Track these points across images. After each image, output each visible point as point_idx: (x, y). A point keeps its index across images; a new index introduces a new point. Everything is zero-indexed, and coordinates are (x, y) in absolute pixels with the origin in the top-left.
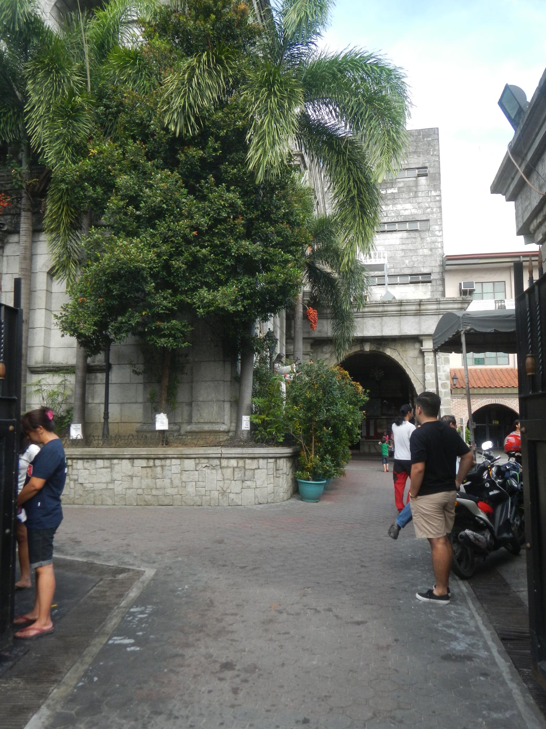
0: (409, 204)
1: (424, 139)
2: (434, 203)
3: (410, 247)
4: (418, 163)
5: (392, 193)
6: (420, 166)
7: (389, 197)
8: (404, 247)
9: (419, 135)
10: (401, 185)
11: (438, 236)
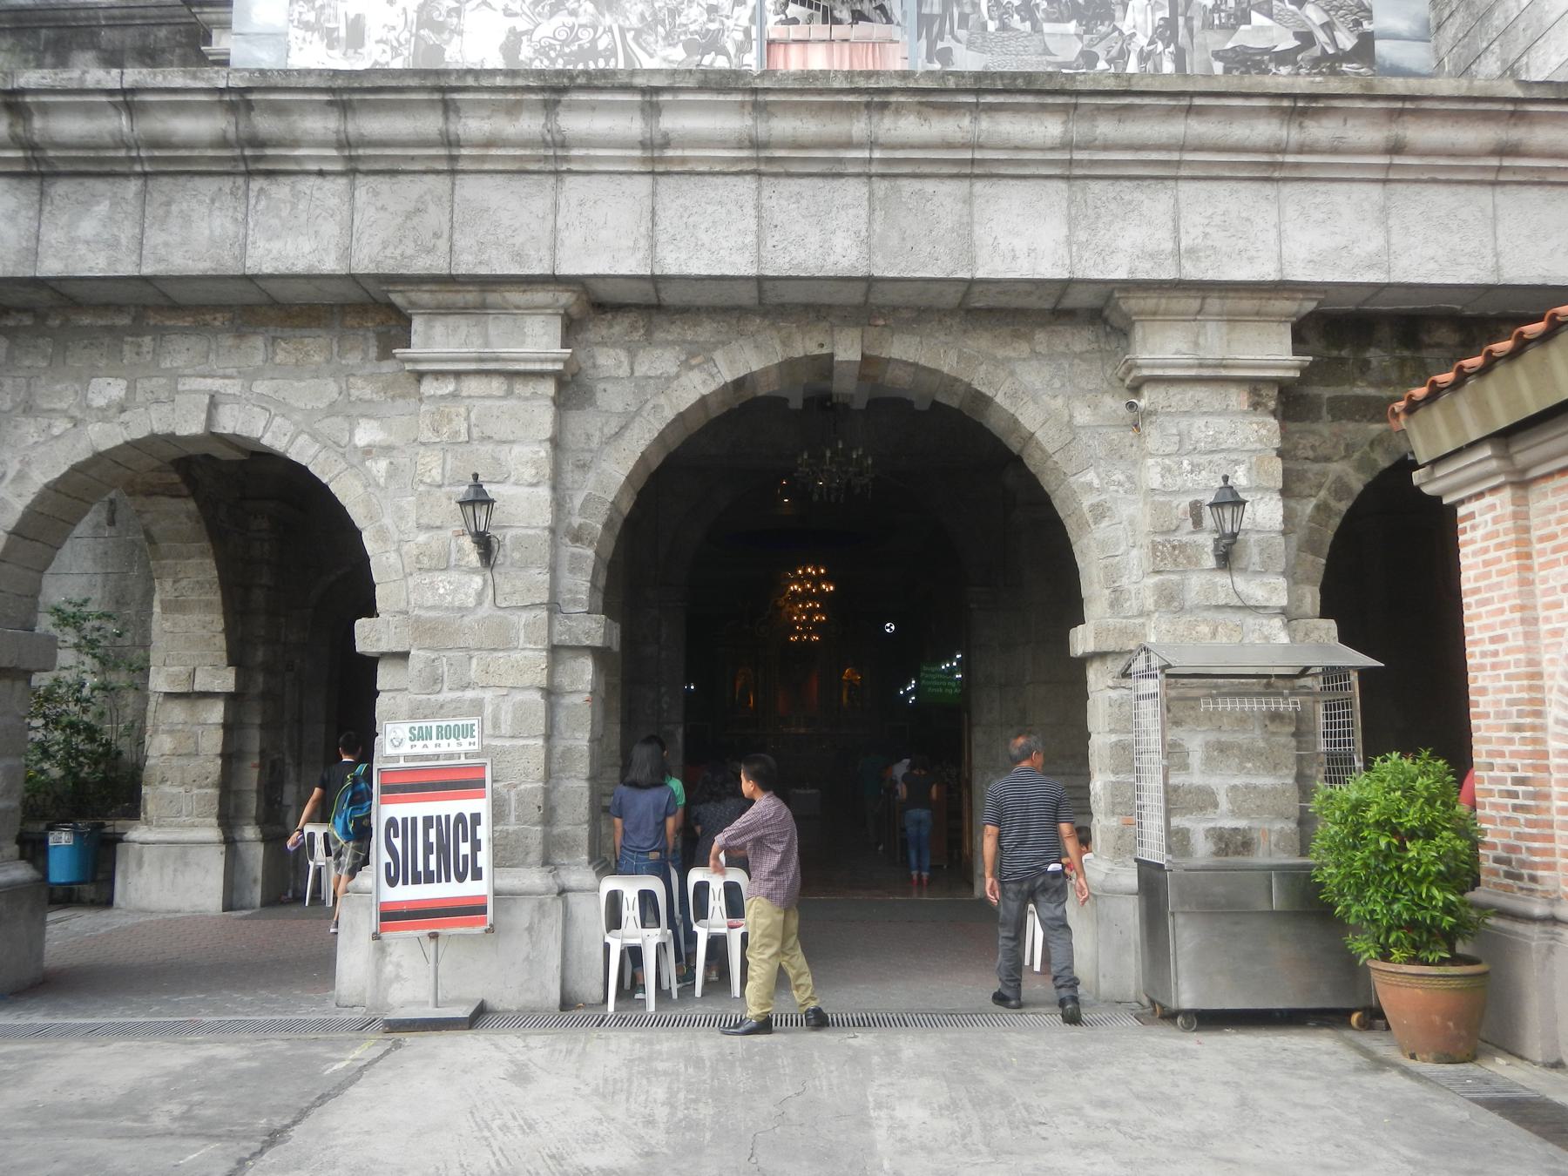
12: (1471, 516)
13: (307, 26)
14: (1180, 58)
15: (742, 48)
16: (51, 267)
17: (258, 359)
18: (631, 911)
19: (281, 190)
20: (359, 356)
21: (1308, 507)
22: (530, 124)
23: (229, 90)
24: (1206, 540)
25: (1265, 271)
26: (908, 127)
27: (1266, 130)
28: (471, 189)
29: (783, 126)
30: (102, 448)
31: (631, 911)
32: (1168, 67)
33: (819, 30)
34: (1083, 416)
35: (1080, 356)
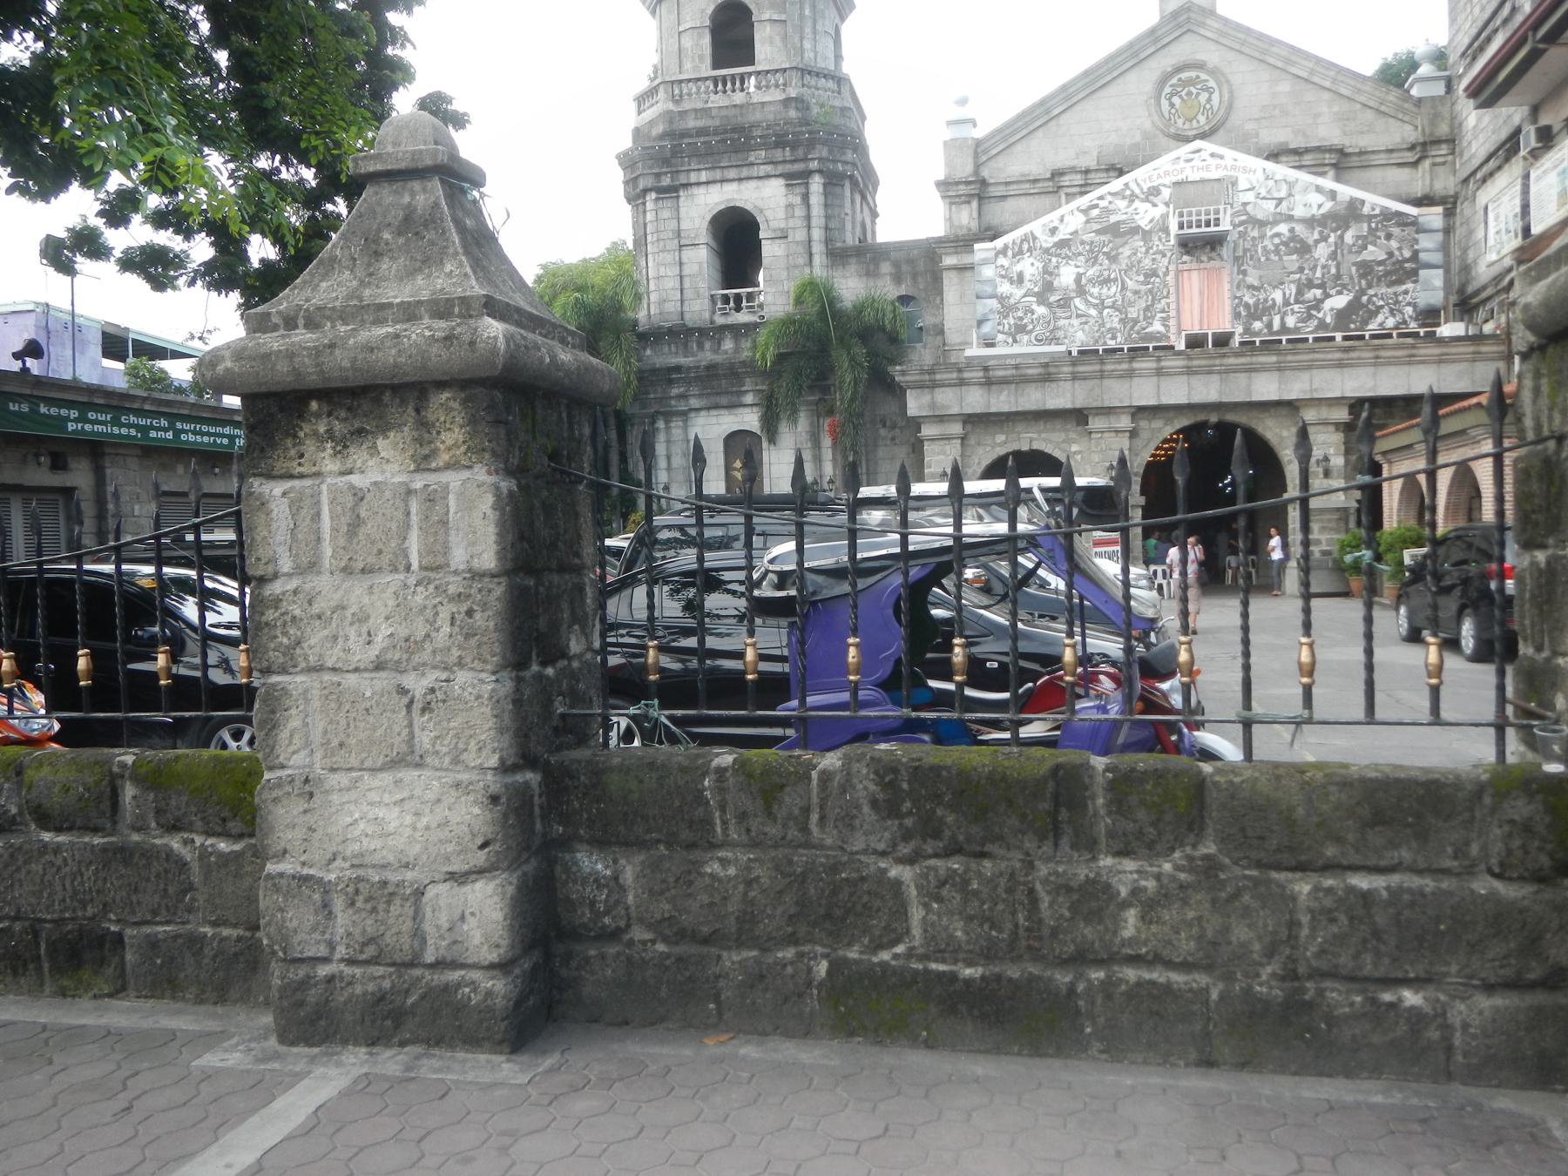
13: (1003, 277)
14: (1338, 267)
15: (1166, 273)
16: (993, 410)
18: (1160, 574)
19: (1054, 385)
20: (1071, 426)
21: (1354, 458)
22: (1125, 366)
24: (1321, 470)
25: (1337, 394)
26: (1232, 361)
27: (1338, 355)
28: (1106, 382)
29: (1196, 363)
31: (1160, 574)
32: (1333, 271)
33: (1194, 265)
34: (1285, 433)
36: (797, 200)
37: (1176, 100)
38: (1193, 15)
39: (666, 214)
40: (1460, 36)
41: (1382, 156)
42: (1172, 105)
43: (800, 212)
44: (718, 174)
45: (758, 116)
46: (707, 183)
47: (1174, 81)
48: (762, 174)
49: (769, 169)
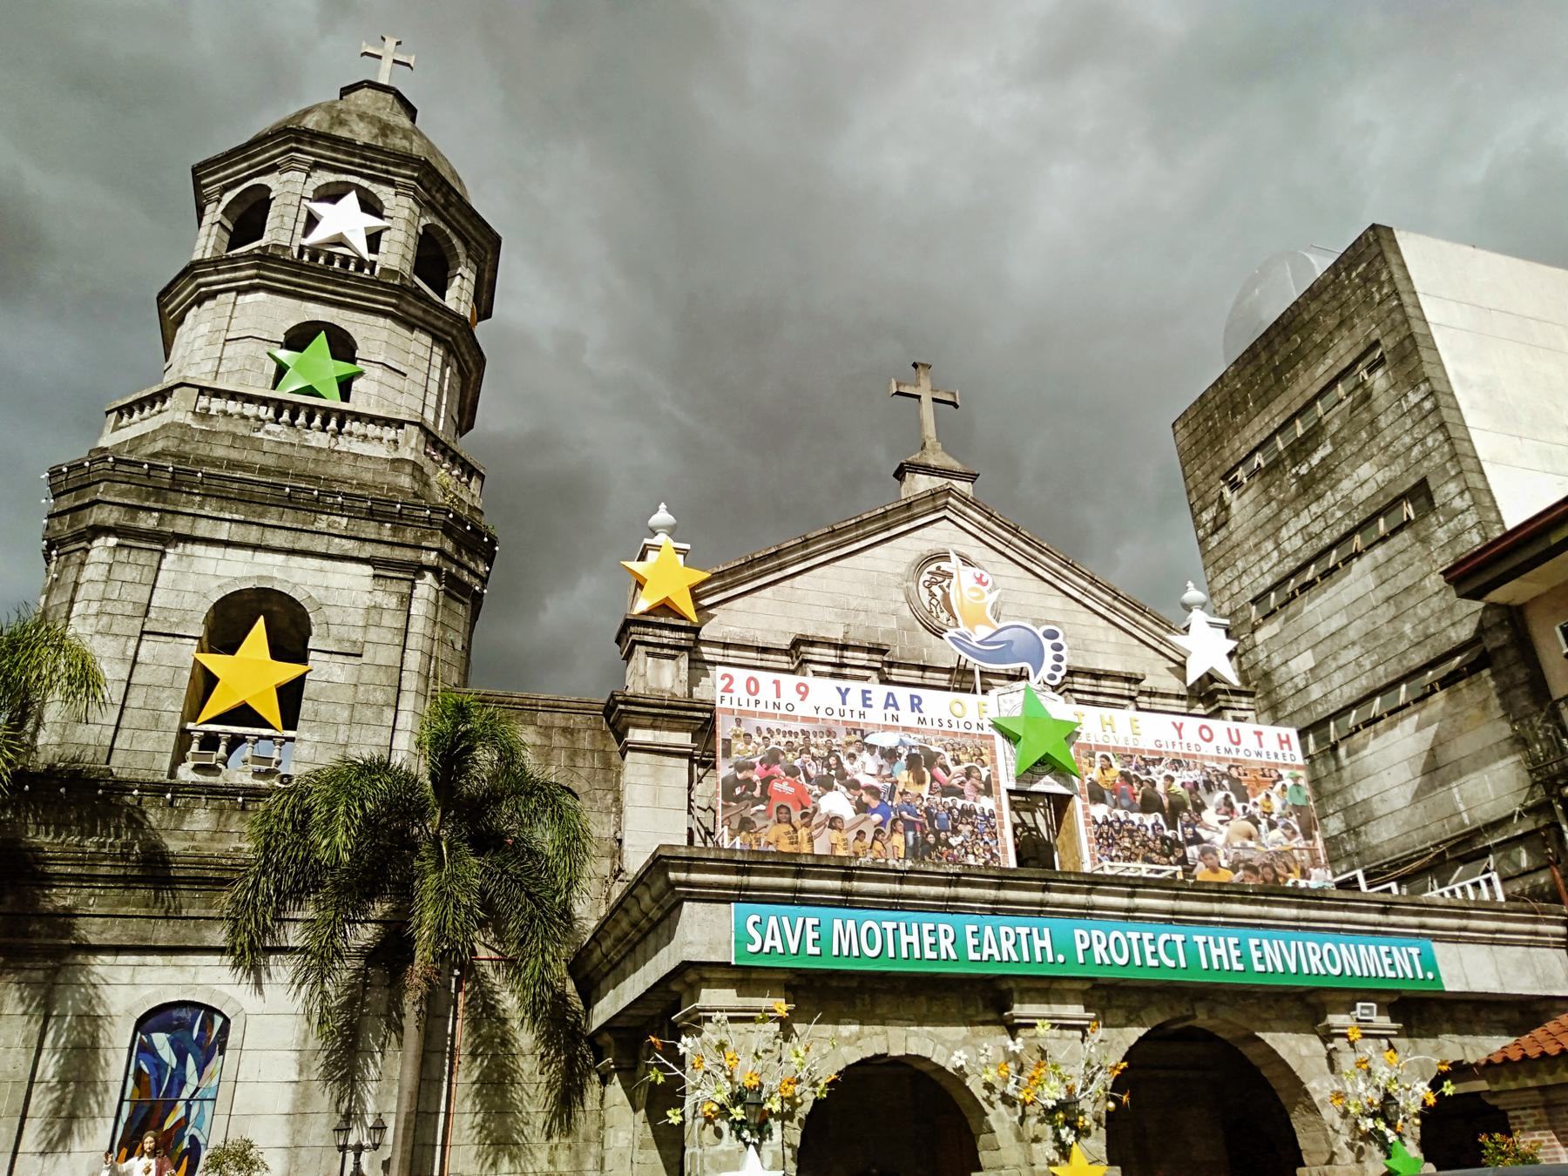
0: (1367, 465)
1: (1348, 276)
2: (1424, 423)
3: (1404, 580)
4: (1356, 345)
5: (1323, 459)
6: (1362, 348)
7: (1318, 476)
8: (1388, 589)
9: (1337, 276)
10: (1333, 428)
11: (1462, 512)
12: (1517, 1117)
17: (924, 1009)
23: (954, 874)
30: (850, 1062)
35: (1298, 1018)
36: (393, 602)
37: (935, 589)
38: (951, 500)
39: (130, 573)
40: (1246, 580)
41: (1174, 701)
42: (933, 595)
43: (393, 620)
44: (253, 535)
45: (345, 471)
46: (227, 544)
47: (932, 568)
48: (332, 551)
49: (349, 546)
